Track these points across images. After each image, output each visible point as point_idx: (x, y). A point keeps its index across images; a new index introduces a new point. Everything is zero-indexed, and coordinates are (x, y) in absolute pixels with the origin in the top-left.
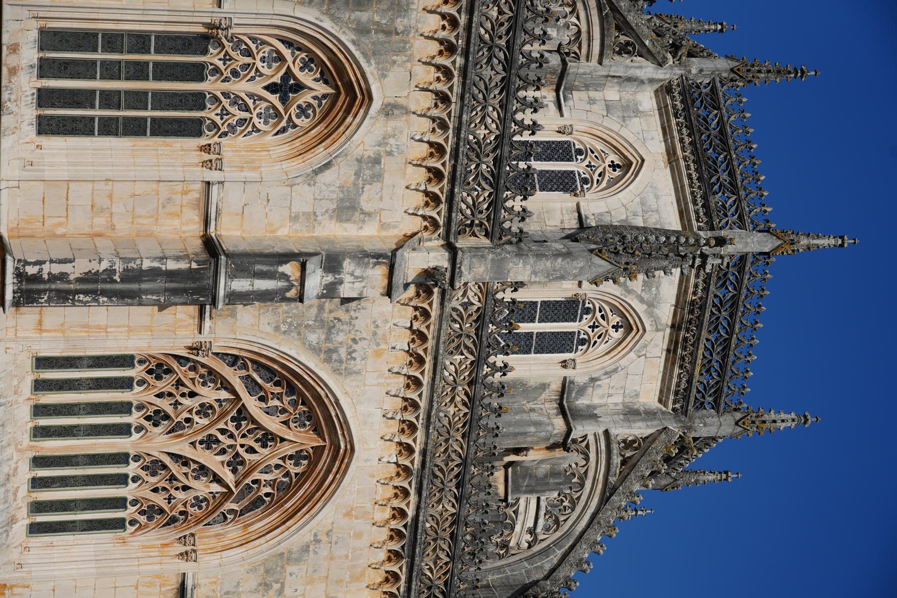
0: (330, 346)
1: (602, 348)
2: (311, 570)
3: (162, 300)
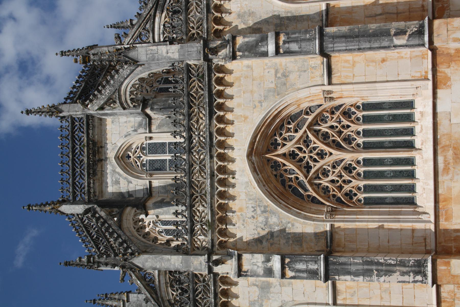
0: (266, 215)
1: (134, 146)
2: (262, 85)
3: (352, 260)
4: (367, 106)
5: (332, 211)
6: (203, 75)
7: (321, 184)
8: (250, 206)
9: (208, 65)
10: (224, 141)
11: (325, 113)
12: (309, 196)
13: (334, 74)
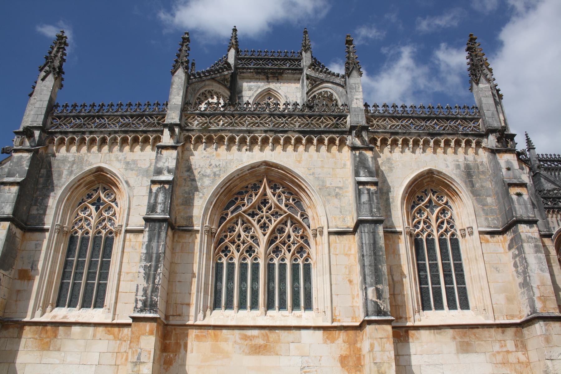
0: (212, 175)
2: (329, 176)
3: (163, 243)
4: (307, 268)
6: (337, 128)
7: (237, 225)
8: (221, 163)
9: (346, 132)
10: (279, 143)
11: (302, 230)
12: (227, 215)
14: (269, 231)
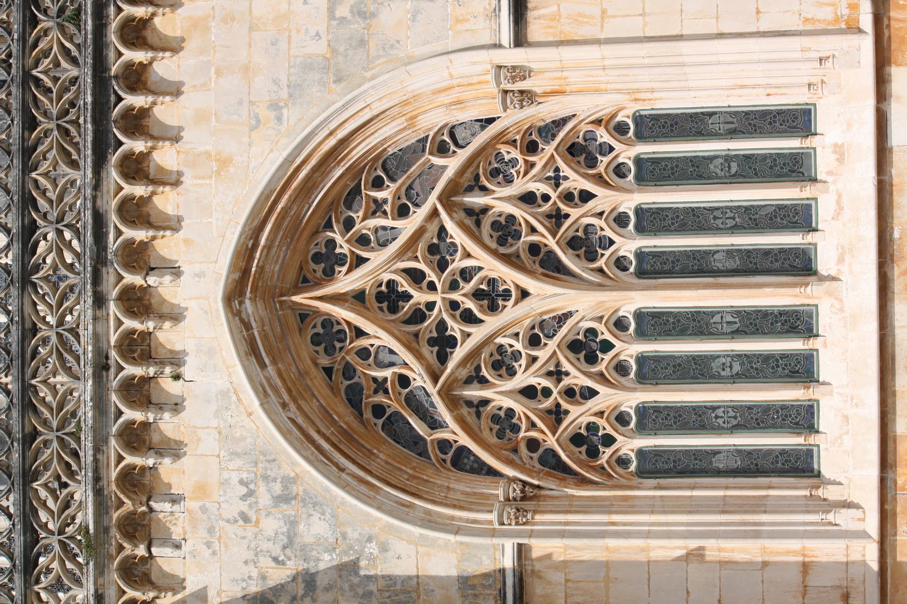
0: (289, 510)
4: (653, 126)
5: (523, 499)
6: (78, 12)
7: (485, 402)
8: (235, 478)
10: (144, 246)
11: (503, 149)
12: (444, 445)
13: (535, 8)
14: (510, 276)
